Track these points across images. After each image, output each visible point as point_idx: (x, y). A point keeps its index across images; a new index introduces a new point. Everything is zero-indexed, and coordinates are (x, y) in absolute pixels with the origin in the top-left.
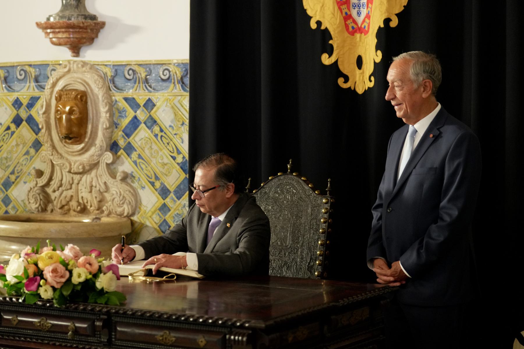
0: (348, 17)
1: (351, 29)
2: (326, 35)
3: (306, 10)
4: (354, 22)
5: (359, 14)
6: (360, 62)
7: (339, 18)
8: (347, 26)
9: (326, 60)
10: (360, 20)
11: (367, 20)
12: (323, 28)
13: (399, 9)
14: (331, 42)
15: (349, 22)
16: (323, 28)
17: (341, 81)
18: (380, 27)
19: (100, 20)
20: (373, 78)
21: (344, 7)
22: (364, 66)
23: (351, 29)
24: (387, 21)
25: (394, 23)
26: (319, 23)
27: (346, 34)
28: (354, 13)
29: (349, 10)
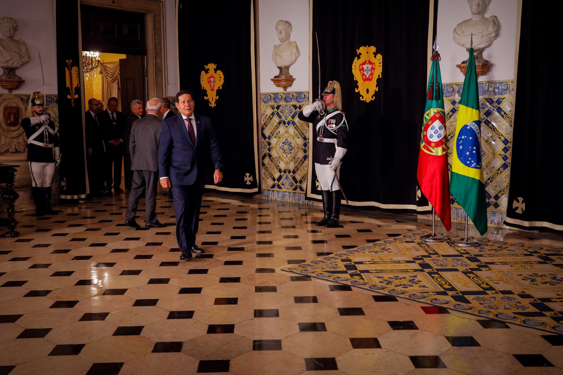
19: (23, 79)
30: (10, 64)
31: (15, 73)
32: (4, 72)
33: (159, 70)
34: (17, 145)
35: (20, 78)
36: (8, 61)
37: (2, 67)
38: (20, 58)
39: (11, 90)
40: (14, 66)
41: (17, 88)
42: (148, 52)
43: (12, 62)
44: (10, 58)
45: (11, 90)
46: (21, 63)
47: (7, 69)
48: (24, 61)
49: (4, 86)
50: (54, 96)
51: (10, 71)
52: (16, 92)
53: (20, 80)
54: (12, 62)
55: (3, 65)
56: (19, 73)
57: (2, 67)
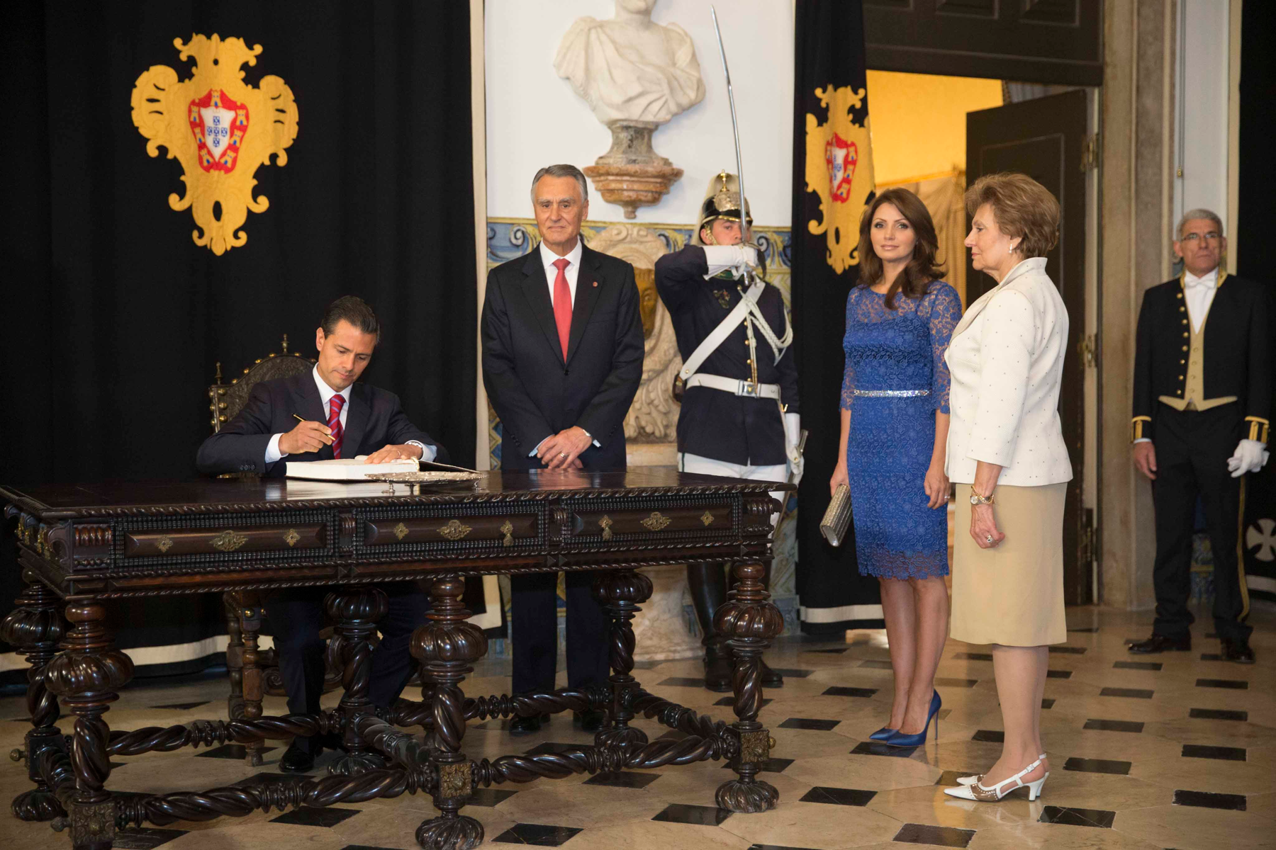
0: (202, 146)
1: (205, 164)
2: (175, 168)
3: (298, 123)
4: (209, 153)
5: (217, 143)
6: (217, 211)
7: (194, 147)
8: (200, 158)
9: (175, 203)
10: (217, 152)
11: (231, 154)
12: (170, 156)
13: (287, 142)
14: (183, 178)
15: (204, 152)
16: (170, 156)
17: (195, 234)
18: (262, 165)
20: (243, 236)
21: (198, 130)
22: (225, 216)
23: (205, 164)
24: (274, 157)
25: (282, 161)
26: (163, 150)
27: (201, 170)
28: (209, 141)
29: (203, 135)
30: (635, 113)
31: (650, 147)
32: (617, 143)
33: (1149, 140)
34: (645, 409)
35: (666, 162)
36: (630, 100)
37: (611, 124)
38: (672, 90)
39: (632, 205)
40: (649, 117)
41: (655, 199)
42: (1109, 72)
43: (643, 102)
44: (635, 89)
45: (632, 205)
46: (674, 108)
47: (627, 128)
48: (685, 101)
49: (612, 191)
50: (778, 231)
51: (638, 135)
52: (646, 215)
53: (667, 169)
54: (643, 102)
55: (616, 115)
56: (667, 147)
57: (611, 124)
